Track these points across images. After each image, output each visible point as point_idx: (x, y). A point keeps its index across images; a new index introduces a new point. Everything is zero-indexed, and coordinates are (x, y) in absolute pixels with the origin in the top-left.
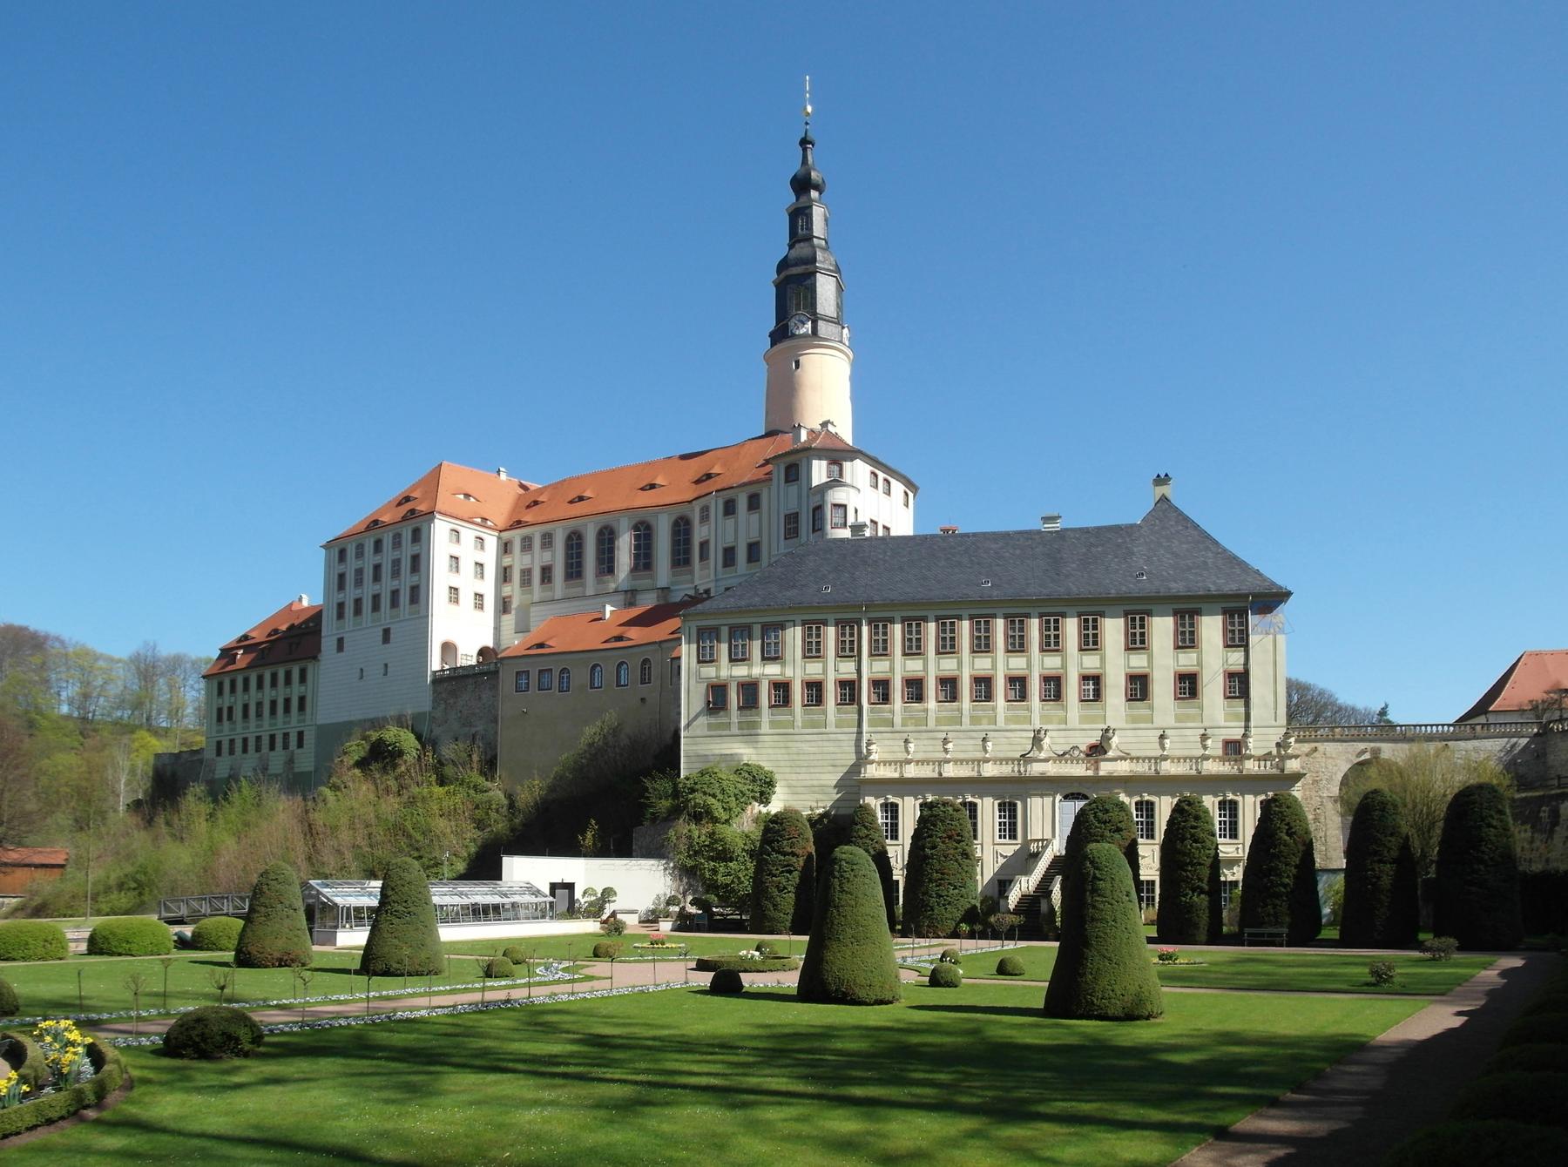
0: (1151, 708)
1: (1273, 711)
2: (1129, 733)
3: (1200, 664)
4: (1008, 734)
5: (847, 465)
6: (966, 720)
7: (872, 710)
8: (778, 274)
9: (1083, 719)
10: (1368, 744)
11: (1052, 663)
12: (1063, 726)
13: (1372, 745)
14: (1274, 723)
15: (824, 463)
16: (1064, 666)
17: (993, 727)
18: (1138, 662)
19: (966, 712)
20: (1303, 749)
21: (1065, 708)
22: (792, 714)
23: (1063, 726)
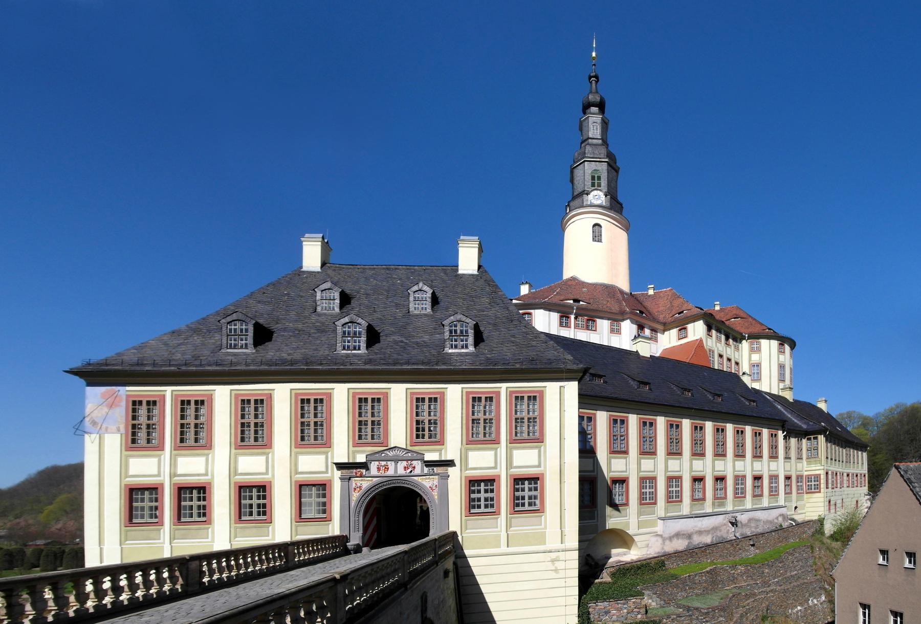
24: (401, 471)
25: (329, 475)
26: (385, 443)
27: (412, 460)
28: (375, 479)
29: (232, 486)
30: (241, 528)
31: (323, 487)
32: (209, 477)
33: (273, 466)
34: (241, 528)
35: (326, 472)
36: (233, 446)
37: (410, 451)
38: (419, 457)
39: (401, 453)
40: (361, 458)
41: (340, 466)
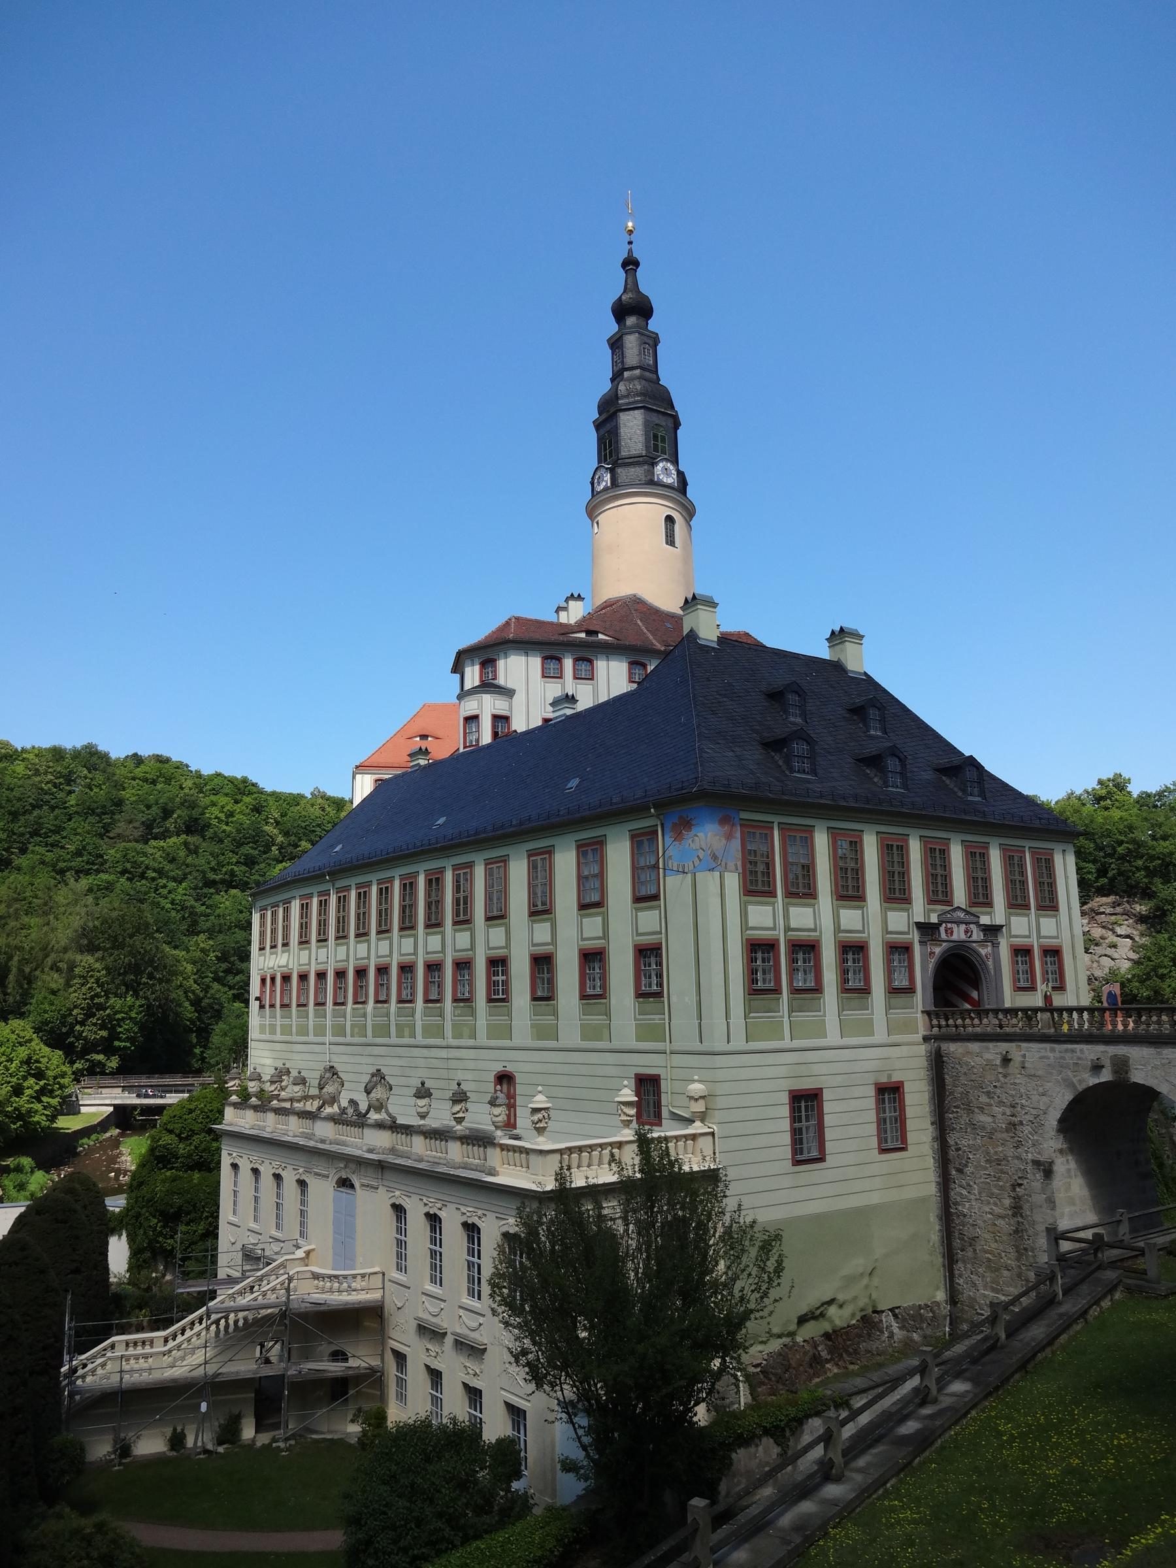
0: (555, 1013)
1: (697, 1022)
2: (537, 1055)
3: (606, 935)
4: (425, 1052)
5: (501, 663)
6: (393, 1029)
7: (334, 1010)
8: (600, 413)
9: (493, 1032)
10: (1101, 1048)
11: (497, 936)
12: (471, 1042)
13: (1113, 1050)
14: (697, 1046)
15: (477, 668)
16: (473, 947)
17: (411, 1041)
18: (542, 932)
19: (392, 1018)
20: (987, 1056)
21: (473, 1013)
22: (290, 1017)
23: (471, 1042)
24: (963, 937)
25: (911, 936)
26: (949, 902)
27: (970, 923)
28: (944, 944)
29: (837, 945)
30: (847, 998)
31: (906, 949)
32: (818, 934)
33: (868, 924)
34: (847, 998)
35: (908, 933)
36: (835, 897)
37: (967, 913)
38: (975, 920)
39: (962, 915)
40: (934, 919)
41: (919, 926)
